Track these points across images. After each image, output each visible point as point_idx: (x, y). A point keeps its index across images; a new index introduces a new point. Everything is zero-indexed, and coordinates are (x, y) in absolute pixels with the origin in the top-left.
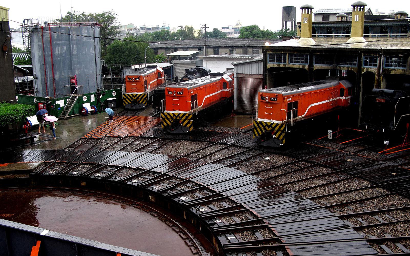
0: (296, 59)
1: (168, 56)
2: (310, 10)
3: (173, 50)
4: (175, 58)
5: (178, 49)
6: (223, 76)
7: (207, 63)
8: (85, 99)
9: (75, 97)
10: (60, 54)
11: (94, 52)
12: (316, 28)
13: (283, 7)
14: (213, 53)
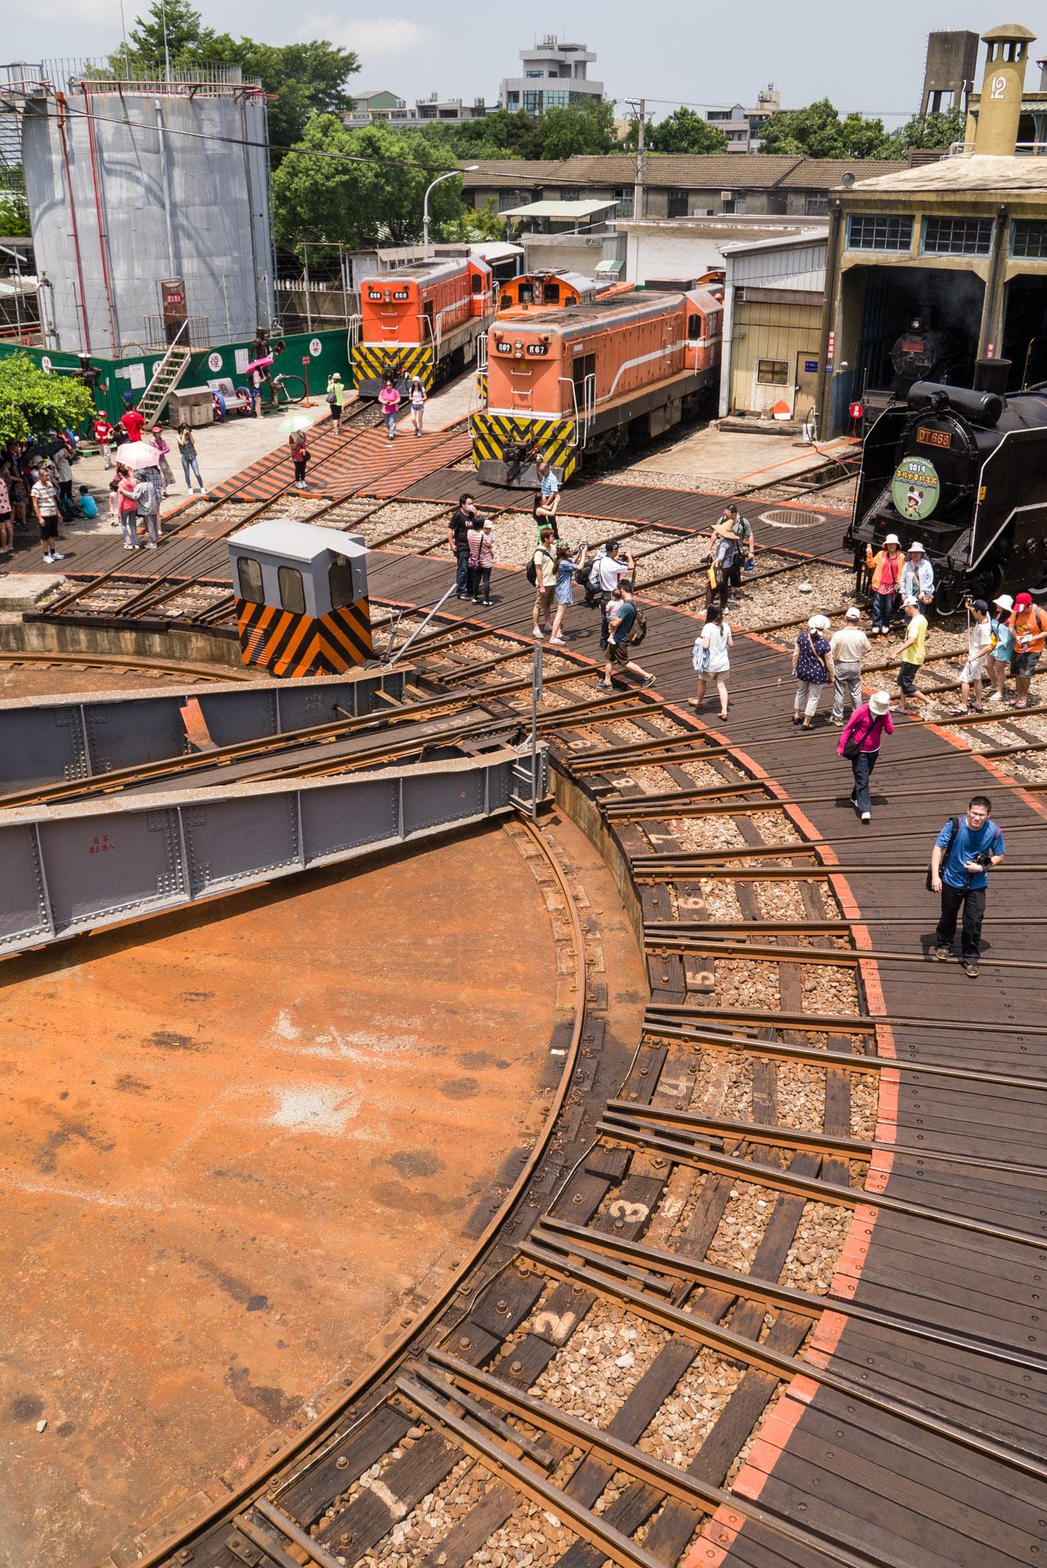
0: (945, 236)
1: (509, 217)
2: (1018, 47)
3: (528, 196)
4: (533, 224)
5: (545, 194)
6: (688, 294)
7: (641, 245)
8: (215, 363)
9: (182, 356)
10: (128, 200)
11: (246, 197)
12: (1038, 116)
13: (932, 36)
14: (665, 211)
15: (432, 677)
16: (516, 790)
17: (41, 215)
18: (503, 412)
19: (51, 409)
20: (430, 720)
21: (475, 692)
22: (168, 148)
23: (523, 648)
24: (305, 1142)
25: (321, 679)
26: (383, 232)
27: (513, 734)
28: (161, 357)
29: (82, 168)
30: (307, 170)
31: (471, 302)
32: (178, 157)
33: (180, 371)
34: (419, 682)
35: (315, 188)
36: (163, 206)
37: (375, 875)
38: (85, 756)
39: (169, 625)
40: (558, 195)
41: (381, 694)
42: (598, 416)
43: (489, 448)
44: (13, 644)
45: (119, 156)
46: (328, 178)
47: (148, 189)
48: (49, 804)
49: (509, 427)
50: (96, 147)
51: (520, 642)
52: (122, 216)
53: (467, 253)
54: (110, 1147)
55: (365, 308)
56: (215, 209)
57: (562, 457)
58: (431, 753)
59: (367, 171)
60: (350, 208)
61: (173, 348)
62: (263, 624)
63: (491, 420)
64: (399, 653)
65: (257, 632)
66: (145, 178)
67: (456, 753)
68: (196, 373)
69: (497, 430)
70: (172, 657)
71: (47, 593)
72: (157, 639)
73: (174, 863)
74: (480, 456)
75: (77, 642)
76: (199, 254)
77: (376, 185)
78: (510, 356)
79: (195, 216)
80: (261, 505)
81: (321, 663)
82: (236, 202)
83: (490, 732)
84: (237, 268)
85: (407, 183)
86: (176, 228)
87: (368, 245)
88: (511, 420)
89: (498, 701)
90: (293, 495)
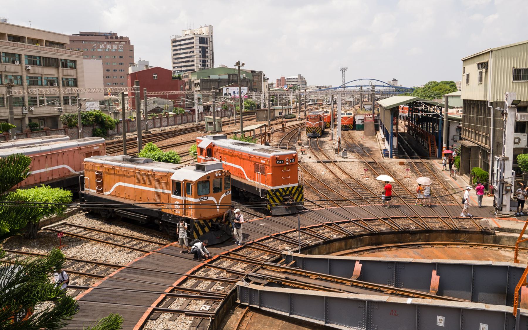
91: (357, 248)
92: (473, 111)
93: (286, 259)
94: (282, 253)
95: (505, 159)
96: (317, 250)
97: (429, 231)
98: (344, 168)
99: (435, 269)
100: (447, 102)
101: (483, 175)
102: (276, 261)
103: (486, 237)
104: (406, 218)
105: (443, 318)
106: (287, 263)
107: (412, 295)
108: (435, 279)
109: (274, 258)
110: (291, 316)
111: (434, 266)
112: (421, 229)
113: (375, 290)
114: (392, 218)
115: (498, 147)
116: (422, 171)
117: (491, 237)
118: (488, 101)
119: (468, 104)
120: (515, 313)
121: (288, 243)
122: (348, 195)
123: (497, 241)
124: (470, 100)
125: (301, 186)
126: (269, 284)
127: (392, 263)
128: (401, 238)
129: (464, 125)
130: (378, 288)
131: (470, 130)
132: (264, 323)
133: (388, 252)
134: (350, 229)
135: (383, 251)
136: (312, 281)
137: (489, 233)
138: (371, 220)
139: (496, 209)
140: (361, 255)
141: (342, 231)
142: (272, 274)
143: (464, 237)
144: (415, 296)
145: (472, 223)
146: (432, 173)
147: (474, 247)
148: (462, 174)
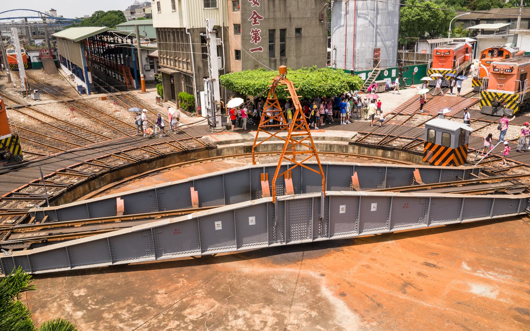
1: (470, 29)
3: (474, 22)
4: (476, 32)
5: (481, 22)
7: (523, 38)
8: (386, 73)
9: (378, 71)
14: (527, 27)
15: (488, 171)
16: (529, 207)
17: (336, 30)
18: (492, 91)
19: (355, 84)
20: (492, 183)
21: (506, 176)
22: (377, 9)
23: (517, 165)
24: (485, 299)
25: (452, 167)
26: (427, 34)
27: (524, 190)
28: (371, 71)
29: (351, 15)
30: (407, 15)
31: (465, 57)
32: (380, 11)
33: (377, 75)
34: (483, 171)
35: (408, 21)
36: (374, 27)
37: (481, 228)
38: (385, 183)
39: (394, 149)
40: (486, 22)
41: (472, 174)
42: (527, 93)
43: (486, 102)
44: (344, 151)
45: (362, 12)
46: (413, 17)
47: (370, 22)
48: (401, 192)
49: (494, 96)
50: (356, 9)
51: (515, 163)
52: (361, 29)
53: (464, 41)
54: (421, 290)
55: (434, 58)
56: (389, 27)
57: (514, 106)
58: (496, 193)
59: (426, 15)
60: (419, 27)
61: (375, 69)
62: (433, 149)
63: (488, 93)
64: (479, 162)
65: (431, 152)
66: (369, 18)
67: (504, 193)
68: (381, 77)
69: (490, 96)
70: (393, 158)
71: (354, 137)
72: (389, 152)
73: (425, 215)
74: (482, 105)
75: (363, 151)
76: (382, 41)
77: (428, 19)
78: (499, 72)
79: (382, 29)
80: (409, 116)
81: (452, 163)
82: (395, 25)
83: (516, 189)
84: (393, 45)
85: (438, 19)
86: (377, 33)
87: (424, 39)
88: (495, 93)
89: (514, 180)
90: (419, 114)
91: (100, 188)
92: (169, 38)
93: (36, 216)
94: (29, 211)
95: (213, 81)
96: (62, 200)
97: (163, 157)
98: (43, 111)
99: (193, 186)
100: (138, 32)
101: (190, 99)
102: (26, 221)
103: (210, 151)
104: (137, 149)
105: (220, 223)
106: (38, 219)
107: (180, 214)
108: (194, 194)
109: (21, 220)
110: (73, 269)
111: (191, 183)
112: (156, 156)
113: (146, 219)
114: (124, 152)
115: (203, 71)
116: (127, 103)
117: (214, 151)
118: (185, 28)
119: (163, 33)
120: (274, 201)
121: (27, 200)
122: (66, 138)
123: (219, 153)
124: (164, 28)
125: (16, 136)
126: (31, 248)
127: (153, 190)
128: (140, 168)
129: (160, 53)
130: (148, 217)
131: (168, 57)
132: (45, 287)
133: (133, 184)
134: (90, 170)
135: (127, 184)
136: (78, 229)
137: (212, 148)
138: (104, 157)
139: (211, 126)
140: (108, 193)
141: (81, 175)
142: (29, 235)
143: (193, 155)
144: (183, 213)
145: (195, 141)
146: (138, 103)
147: (204, 162)
148: (166, 101)
